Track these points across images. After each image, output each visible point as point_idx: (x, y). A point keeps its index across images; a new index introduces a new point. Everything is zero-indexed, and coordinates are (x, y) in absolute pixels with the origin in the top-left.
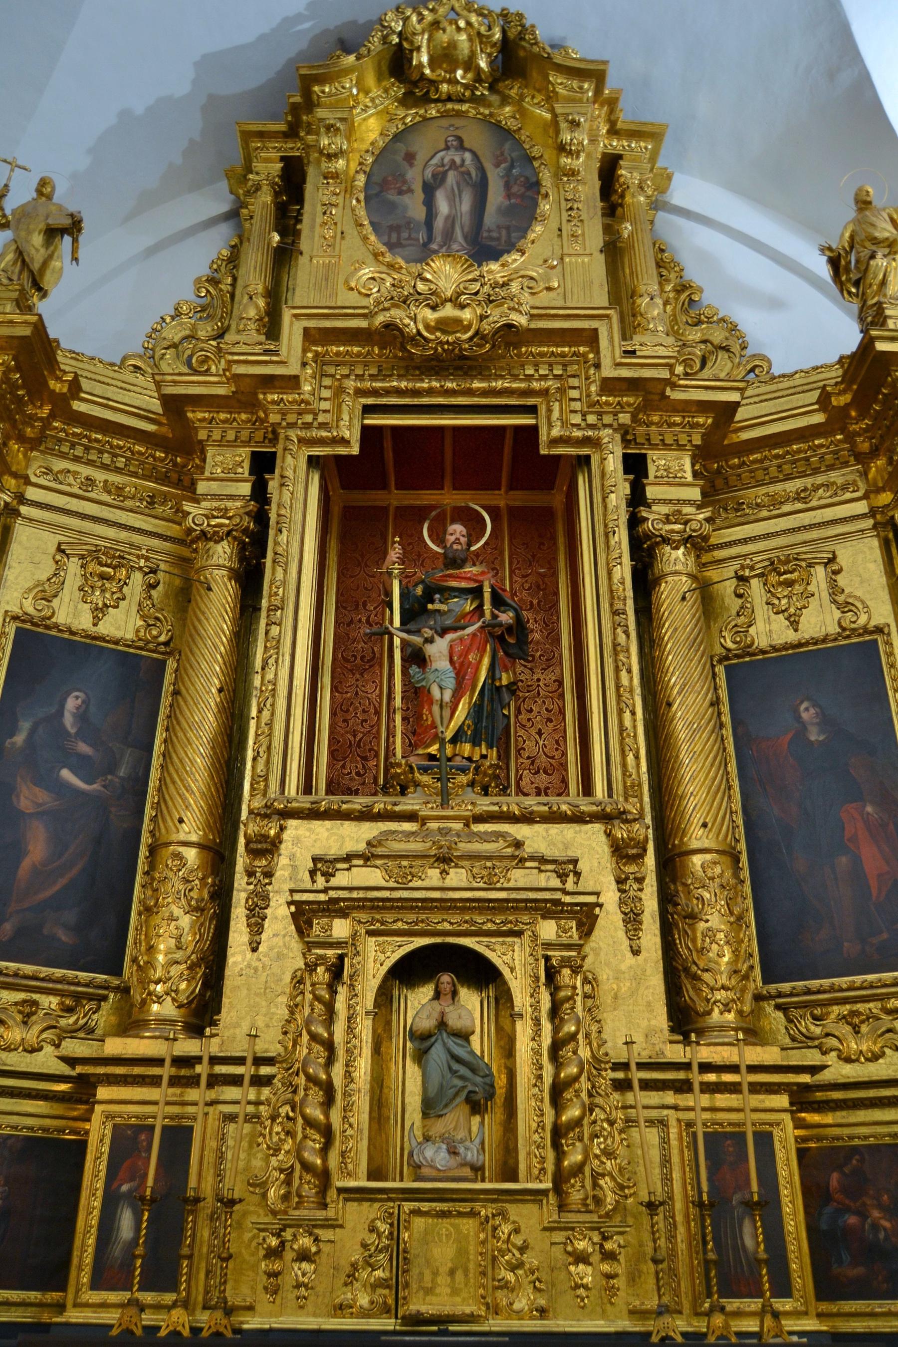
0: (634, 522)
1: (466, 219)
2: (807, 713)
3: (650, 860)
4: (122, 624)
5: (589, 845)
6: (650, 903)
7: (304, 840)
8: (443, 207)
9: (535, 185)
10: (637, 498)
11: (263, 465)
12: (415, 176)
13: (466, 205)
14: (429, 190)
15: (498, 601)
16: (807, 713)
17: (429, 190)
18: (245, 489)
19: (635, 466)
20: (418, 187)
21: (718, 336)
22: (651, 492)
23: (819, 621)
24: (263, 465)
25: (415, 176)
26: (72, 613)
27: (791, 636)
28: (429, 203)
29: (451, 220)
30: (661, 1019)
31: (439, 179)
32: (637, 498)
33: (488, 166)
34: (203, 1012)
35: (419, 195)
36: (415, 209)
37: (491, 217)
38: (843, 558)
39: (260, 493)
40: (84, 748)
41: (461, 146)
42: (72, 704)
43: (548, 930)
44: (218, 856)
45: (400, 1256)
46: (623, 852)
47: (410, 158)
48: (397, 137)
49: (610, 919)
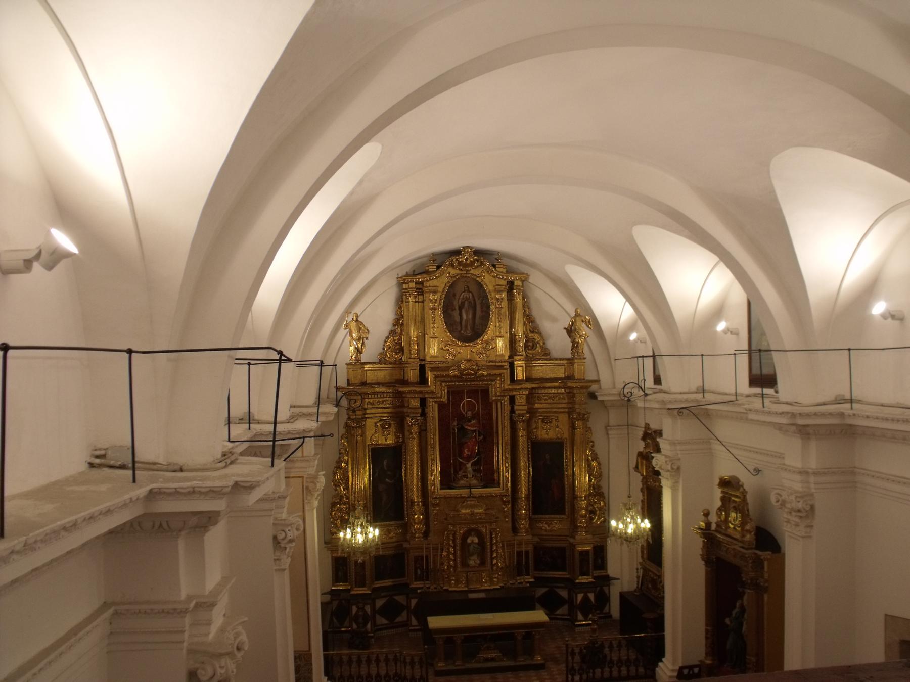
1: (470, 322)
2: (547, 457)
10: (512, 411)
11: (423, 402)
12: (456, 304)
13: (470, 316)
14: (460, 308)
16: (547, 457)
17: (460, 308)
18: (420, 411)
20: (457, 307)
21: (537, 337)
22: (516, 408)
24: (423, 402)
25: (456, 304)
27: (546, 436)
28: (460, 314)
29: (467, 321)
31: (463, 303)
32: (512, 411)
33: (476, 299)
35: (458, 312)
36: (456, 314)
37: (477, 321)
38: (560, 419)
39: (423, 414)
40: (389, 473)
41: (469, 291)
42: (385, 463)
47: (454, 295)
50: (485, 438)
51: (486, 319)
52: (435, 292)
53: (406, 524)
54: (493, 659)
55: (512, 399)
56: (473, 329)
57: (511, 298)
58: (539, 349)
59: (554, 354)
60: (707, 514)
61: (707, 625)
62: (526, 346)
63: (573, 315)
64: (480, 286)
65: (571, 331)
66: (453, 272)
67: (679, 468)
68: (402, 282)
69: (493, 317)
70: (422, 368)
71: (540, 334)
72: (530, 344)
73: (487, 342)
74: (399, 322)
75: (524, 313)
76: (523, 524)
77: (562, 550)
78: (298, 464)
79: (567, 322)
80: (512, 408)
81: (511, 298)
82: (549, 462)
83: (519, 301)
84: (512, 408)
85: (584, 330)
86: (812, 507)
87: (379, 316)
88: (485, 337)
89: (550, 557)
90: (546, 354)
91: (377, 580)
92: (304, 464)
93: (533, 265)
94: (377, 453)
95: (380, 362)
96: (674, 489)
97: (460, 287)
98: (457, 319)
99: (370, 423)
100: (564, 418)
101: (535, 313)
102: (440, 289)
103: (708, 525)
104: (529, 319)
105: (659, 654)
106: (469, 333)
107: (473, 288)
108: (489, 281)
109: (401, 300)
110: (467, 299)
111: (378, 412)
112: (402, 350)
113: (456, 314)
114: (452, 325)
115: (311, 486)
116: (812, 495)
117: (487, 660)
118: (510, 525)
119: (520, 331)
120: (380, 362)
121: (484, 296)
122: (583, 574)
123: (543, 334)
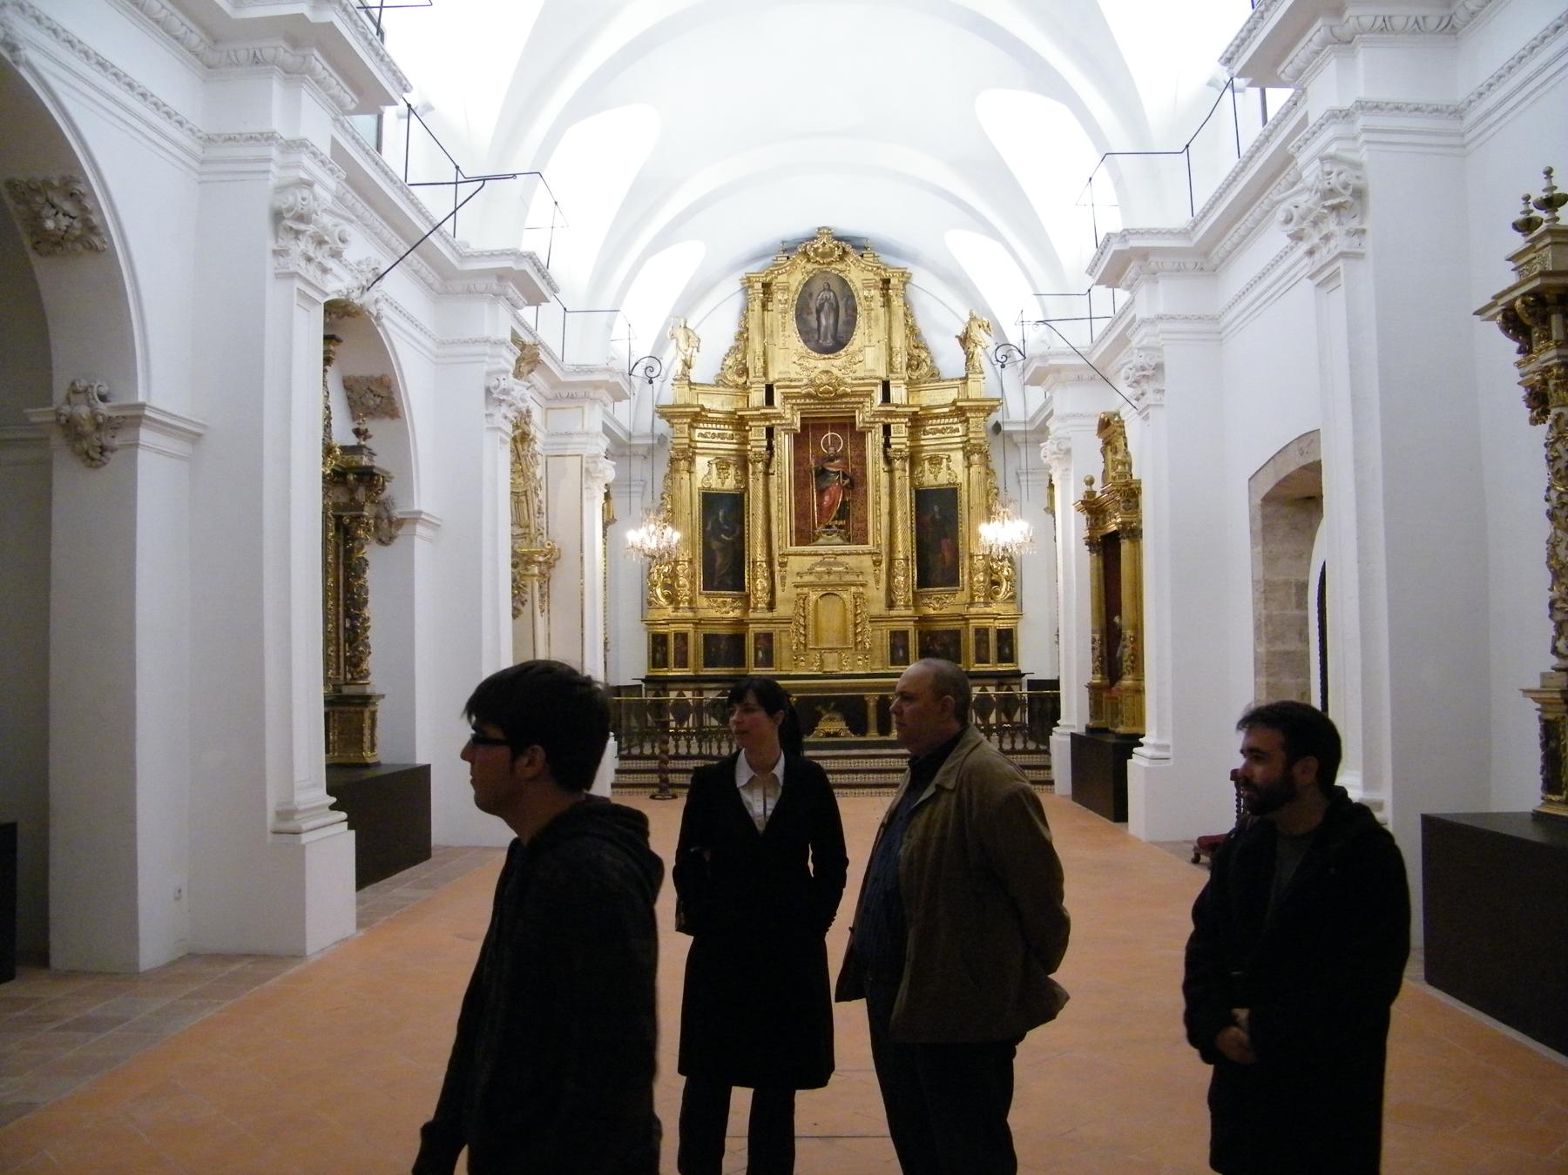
0: (885, 452)
2: (936, 509)
3: (884, 566)
4: (730, 484)
5: (867, 561)
6: (883, 577)
7: (795, 564)
8: (823, 322)
9: (855, 310)
10: (887, 445)
11: (770, 432)
12: (813, 306)
13: (831, 321)
14: (818, 312)
15: (845, 476)
16: (936, 509)
17: (818, 312)
19: (887, 429)
21: (924, 355)
23: (943, 479)
24: (770, 432)
25: (813, 306)
26: (715, 483)
28: (818, 319)
30: (883, 606)
31: (822, 305)
32: (887, 445)
34: (771, 606)
36: (812, 319)
39: (770, 447)
43: (853, 589)
44: (770, 563)
45: (822, 661)
46: (877, 563)
48: (807, 284)
49: (872, 583)
50: (852, 483)
51: (852, 323)
52: (786, 289)
53: (748, 596)
54: (836, 735)
55: (887, 429)
56: (834, 337)
57: (887, 303)
58: (925, 369)
59: (944, 375)
60: (1090, 482)
61: (1093, 632)
62: (909, 366)
63: (967, 319)
64: (844, 282)
65: (964, 340)
66: (810, 267)
67: (1068, 452)
68: (747, 284)
69: (861, 321)
70: (769, 390)
71: (926, 349)
72: (913, 364)
73: (853, 354)
74: (743, 336)
75: (906, 324)
76: (901, 596)
77: (957, 633)
78: (576, 439)
79: (960, 331)
80: (887, 440)
81: (887, 303)
82: (938, 519)
83: (897, 303)
84: (887, 440)
85: (979, 334)
86: (1159, 368)
87: (717, 327)
88: (850, 348)
89: (938, 641)
90: (935, 375)
91: (706, 665)
92: (584, 439)
93: (914, 259)
94: (710, 500)
95: (717, 385)
96: (1064, 478)
97: (818, 286)
98: (814, 324)
99: (701, 462)
100: (958, 456)
101: (922, 324)
102: (793, 288)
103: (1091, 494)
104: (913, 331)
105: (1056, 714)
106: (829, 343)
107: (835, 286)
108: (857, 275)
109: (746, 311)
110: (827, 300)
111: (713, 443)
112: (744, 371)
113: (812, 319)
114: (806, 333)
115: (592, 467)
116: (1159, 349)
117: (828, 735)
118: (882, 594)
119: (899, 341)
120: (717, 385)
121: (850, 296)
122: (980, 660)
123: (930, 345)
